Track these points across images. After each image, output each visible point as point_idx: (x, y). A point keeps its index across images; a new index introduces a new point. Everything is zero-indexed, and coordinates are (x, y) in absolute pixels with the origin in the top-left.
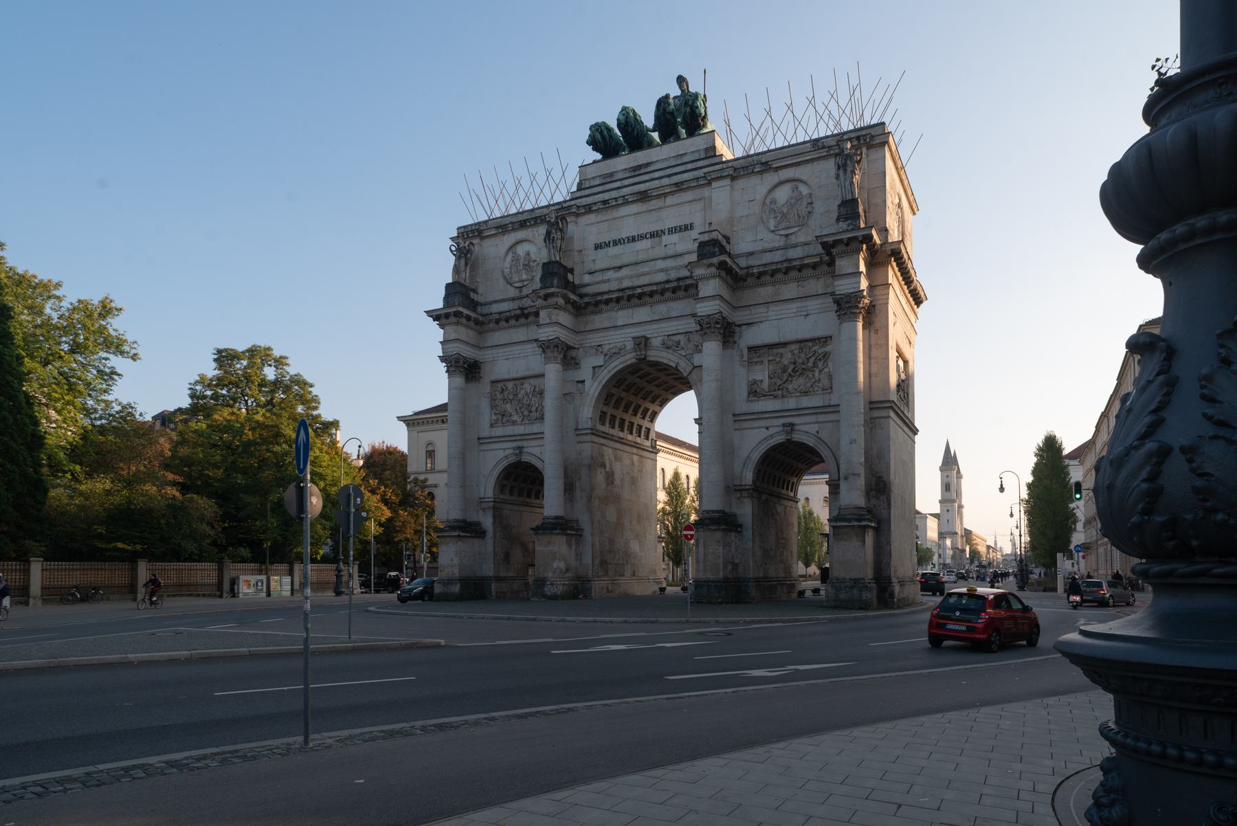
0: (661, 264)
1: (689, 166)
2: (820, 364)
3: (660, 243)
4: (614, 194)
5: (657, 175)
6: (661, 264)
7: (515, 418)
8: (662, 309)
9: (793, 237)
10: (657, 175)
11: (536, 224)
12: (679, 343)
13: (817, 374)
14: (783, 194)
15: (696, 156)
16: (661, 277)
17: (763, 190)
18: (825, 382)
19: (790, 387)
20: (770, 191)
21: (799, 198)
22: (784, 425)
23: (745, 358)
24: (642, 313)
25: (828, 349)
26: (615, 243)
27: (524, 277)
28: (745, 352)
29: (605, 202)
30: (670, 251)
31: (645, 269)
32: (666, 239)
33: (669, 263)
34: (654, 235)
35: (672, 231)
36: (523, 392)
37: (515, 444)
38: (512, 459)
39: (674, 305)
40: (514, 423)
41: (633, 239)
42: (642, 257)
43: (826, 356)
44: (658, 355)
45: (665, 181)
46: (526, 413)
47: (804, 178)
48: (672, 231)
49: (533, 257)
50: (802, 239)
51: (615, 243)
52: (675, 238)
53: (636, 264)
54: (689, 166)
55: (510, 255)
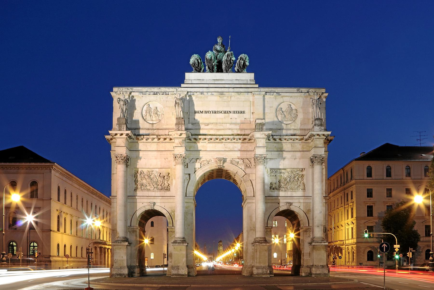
0: (228, 126)
1: (243, 86)
2: (300, 179)
3: (229, 116)
4: (205, 90)
5: (227, 86)
6: (228, 125)
7: (148, 188)
8: (230, 146)
9: (289, 126)
10: (227, 86)
11: (163, 94)
12: (238, 163)
13: (299, 183)
14: (284, 107)
15: (245, 82)
16: (230, 132)
17: (277, 104)
18: (302, 187)
19: (288, 187)
20: (279, 105)
21: (292, 109)
22: (287, 203)
23: (269, 173)
24: (220, 146)
25: (304, 173)
26: (206, 112)
27: (154, 119)
28: (269, 170)
29: (202, 93)
30: (234, 121)
31: (221, 127)
32: (231, 115)
33: (233, 126)
34: (225, 112)
35: (235, 112)
36: (153, 175)
37: (149, 201)
38: (148, 208)
39: (236, 145)
40: (149, 190)
41: (215, 113)
42: (219, 121)
43: (303, 176)
44: (227, 166)
45: (231, 90)
46: (155, 186)
47: (294, 103)
48: (235, 112)
49: (159, 110)
50: (293, 127)
51: (206, 112)
52: (236, 115)
53: (217, 123)
54: (243, 86)
55: (145, 107)
